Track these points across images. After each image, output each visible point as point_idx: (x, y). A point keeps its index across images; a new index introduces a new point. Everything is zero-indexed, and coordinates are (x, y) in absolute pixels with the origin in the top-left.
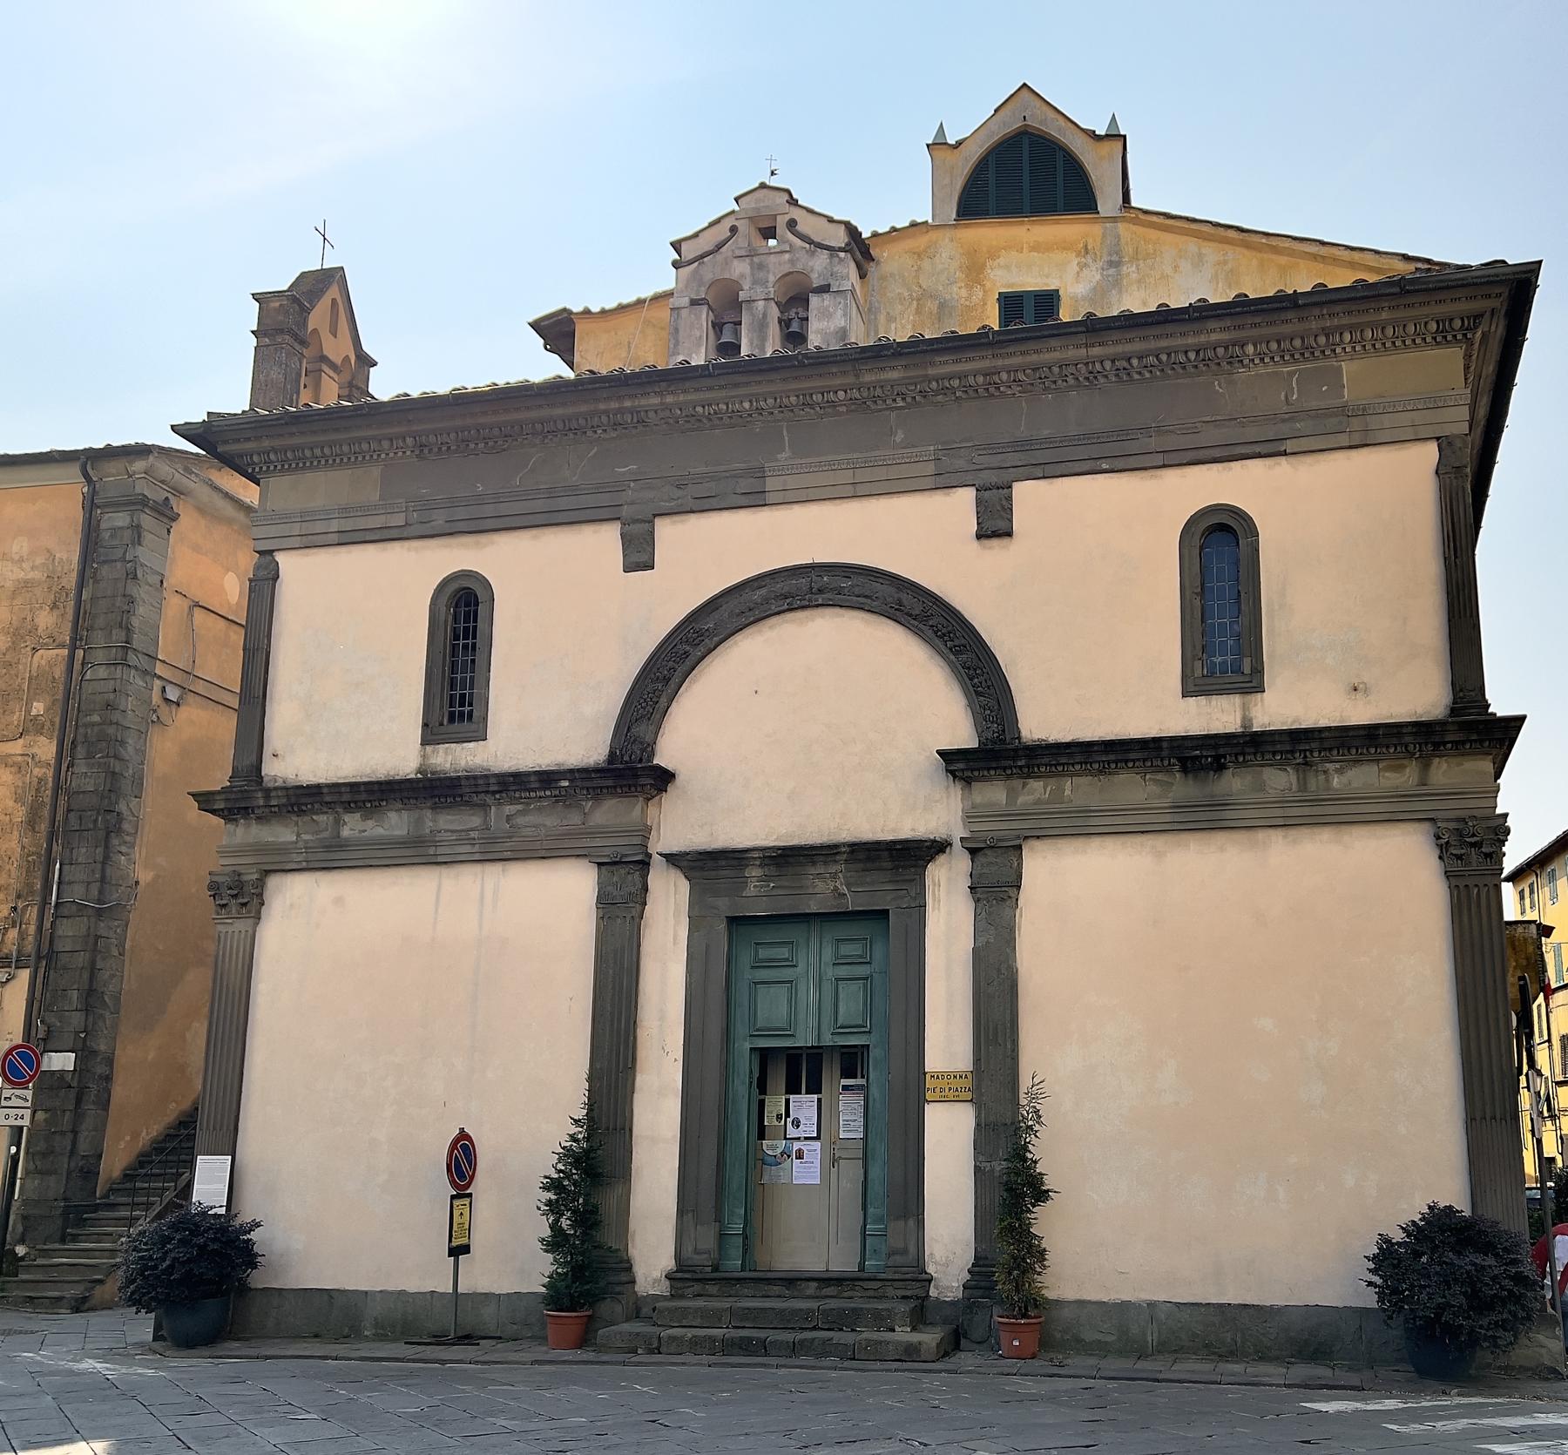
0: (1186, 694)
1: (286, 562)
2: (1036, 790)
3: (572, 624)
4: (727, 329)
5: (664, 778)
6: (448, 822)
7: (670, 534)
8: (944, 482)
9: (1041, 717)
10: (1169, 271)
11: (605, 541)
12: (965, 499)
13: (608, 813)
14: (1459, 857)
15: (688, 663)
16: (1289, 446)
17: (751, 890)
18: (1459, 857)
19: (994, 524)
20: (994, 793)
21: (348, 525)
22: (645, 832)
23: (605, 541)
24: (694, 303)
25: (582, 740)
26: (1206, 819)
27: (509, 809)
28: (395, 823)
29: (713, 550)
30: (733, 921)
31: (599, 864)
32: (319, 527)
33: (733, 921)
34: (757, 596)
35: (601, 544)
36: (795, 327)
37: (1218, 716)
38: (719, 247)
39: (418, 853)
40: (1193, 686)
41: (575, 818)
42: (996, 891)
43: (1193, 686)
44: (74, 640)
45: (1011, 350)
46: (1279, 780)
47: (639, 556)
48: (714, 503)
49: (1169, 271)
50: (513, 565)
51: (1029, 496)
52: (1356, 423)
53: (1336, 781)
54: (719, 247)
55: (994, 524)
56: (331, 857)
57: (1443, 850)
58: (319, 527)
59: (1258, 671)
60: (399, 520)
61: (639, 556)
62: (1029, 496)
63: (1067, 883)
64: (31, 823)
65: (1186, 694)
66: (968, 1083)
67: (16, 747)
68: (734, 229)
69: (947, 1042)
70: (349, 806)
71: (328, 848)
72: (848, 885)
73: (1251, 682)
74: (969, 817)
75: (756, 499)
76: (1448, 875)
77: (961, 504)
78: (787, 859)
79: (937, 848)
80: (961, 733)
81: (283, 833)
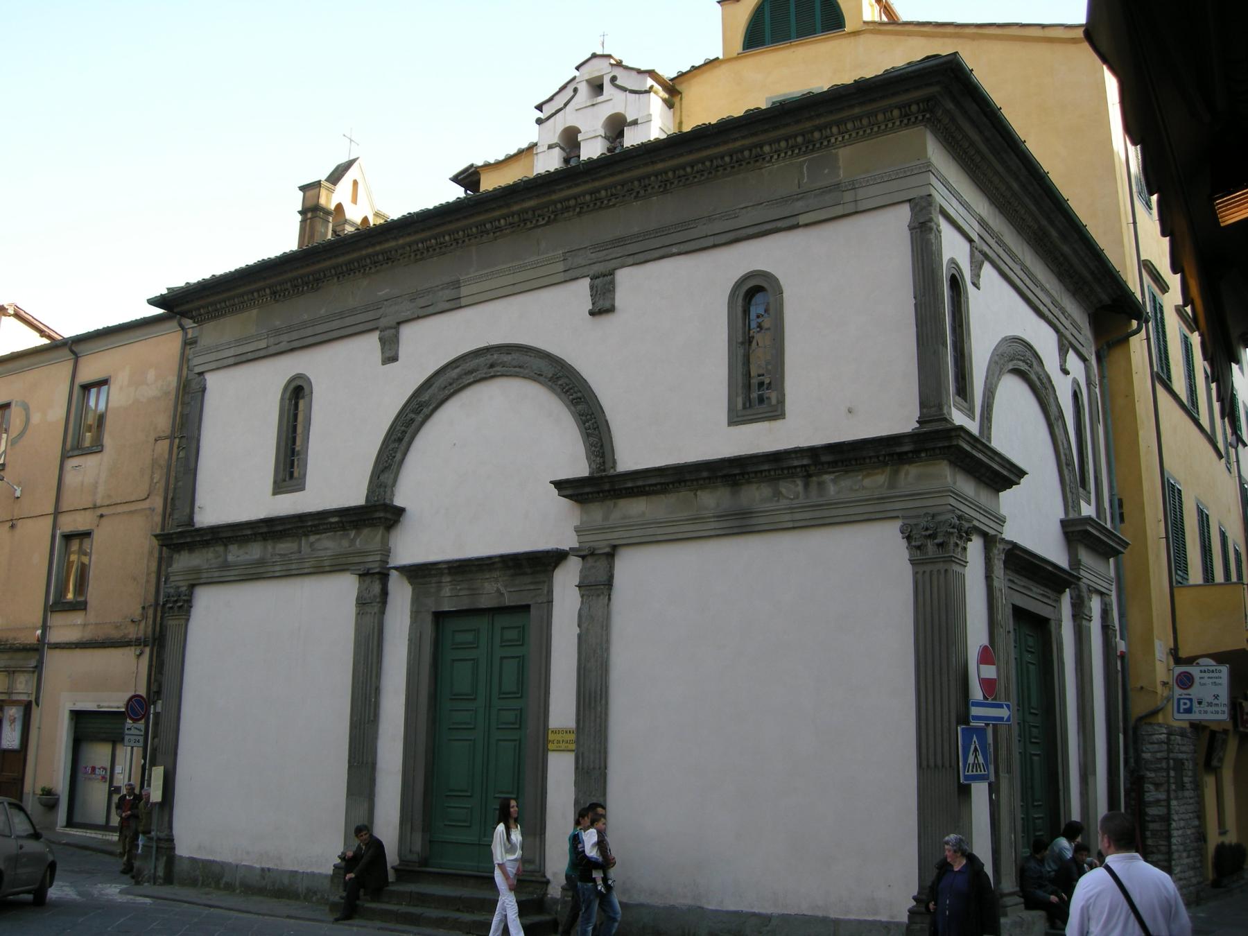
0: (731, 423)
5: (401, 511)
11: (371, 343)
12: (583, 287)
13: (367, 540)
14: (918, 548)
15: (414, 426)
16: (802, 219)
18: (918, 548)
19: (602, 307)
20: (597, 513)
22: (386, 552)
23: (371, 343)
26: (740, 524)
29: (433, 342)
30: (439, 617)
31: (360, 575)
40: (736, 418)
41: (345, 543)
42: (598, 588)
43: (736, 418)
45: (602, 174)
46: (792, 489)
48: (431, 310)
51: (629, 281)
52: (848, 196)
53: (832, 489)
55: (602, 307)
59: (781, 401)
62: (629, 281)
66: (573, 737)
72: (506, 586)
73: (776, 412)
75: (455, 305)
76: (913, 562)
77: (579, 293)
80: (580, 468)
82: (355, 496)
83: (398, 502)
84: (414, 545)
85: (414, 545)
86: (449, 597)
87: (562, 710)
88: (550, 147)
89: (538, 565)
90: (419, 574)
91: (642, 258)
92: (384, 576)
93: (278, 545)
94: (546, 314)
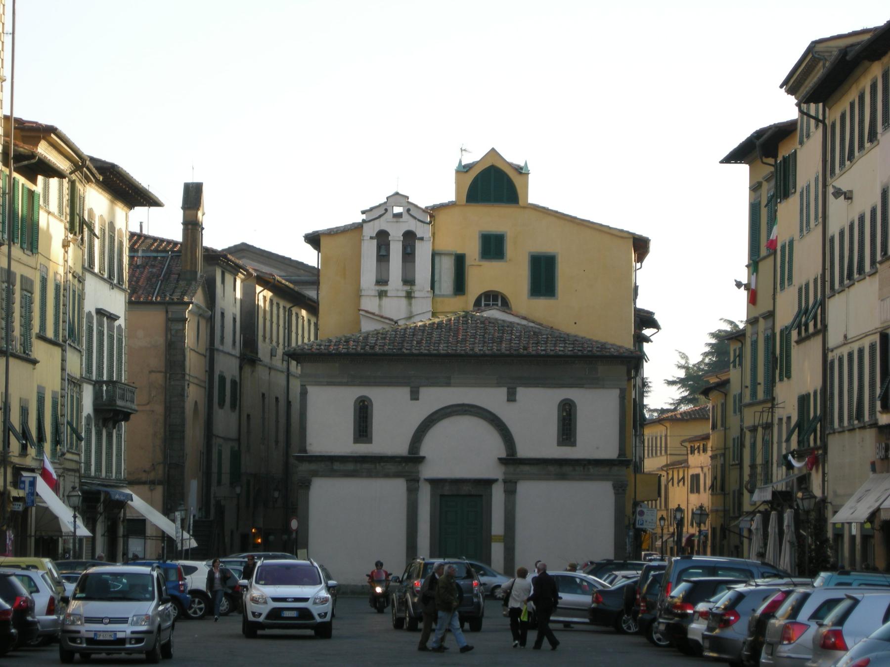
1: (310, 389)
3: (397, 414)
4: (383, 247)
5: (424, 458)
7: (424, 392)
8: (498, 385)
9: (524, 451)
11: (405, 392)
19: (512, 397)
24: (371, 238)
25: (401, 448)
26: (563, 477)
28: (350, 466)
29: (436, 397)
33: (442, 496)
34: (449, 410)
36: (409, 250)
38: (380, 216)
42: (510, 491)
47: (415, 396)
51: (521, 392)
53: (592, 470)
54: (380, 216)
55: (512, 397)
56: (332, 474)
57: (614, 487)
60: (345, 380)
61: (415, 396)
62: (521, 392)
63: (531, 492)
67: (148, 408)
69: (497, 527)
73: (573, 444)
74: (505, 473)
75: (448, 384)
77: (502, 392)
79: (496, 481)
83: (422, 454)
84: (429, 471)
85: (429, 471)
86: (447, 490)
89: (488, 483)
92: (418, 481)
94: (492, 397)
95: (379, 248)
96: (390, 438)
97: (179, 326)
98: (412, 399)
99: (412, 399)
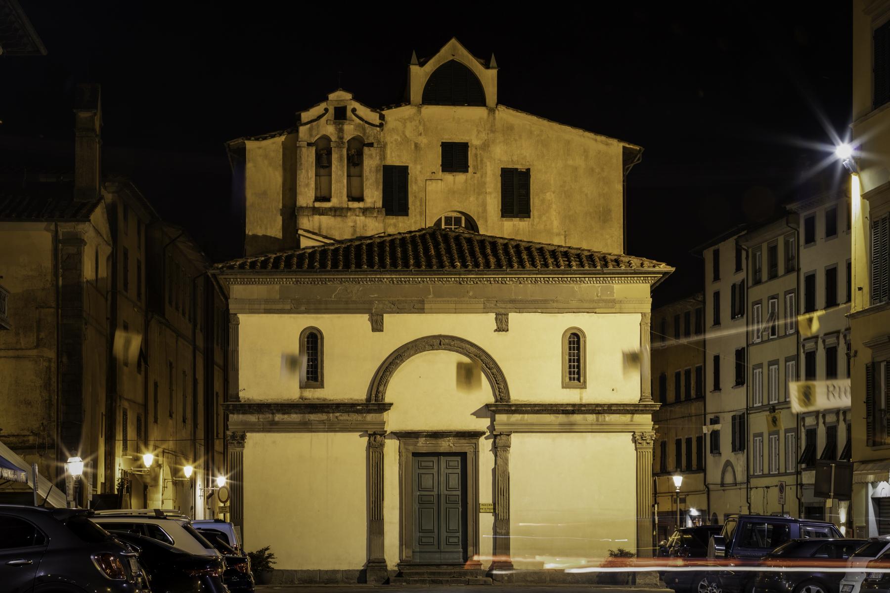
2: (516, 418)
6: (313, 417)
8: (486, 310)
9: (517, 395)
10: (517, 138)
16: (597, 310)
17: (420, 444)
19: (502, 327)
21: (268, 307)
22: (383, 423)
24: (309, 145)
27: (338, 414)
28: (295, 417)
29: (404, 327)
30: (415, 454)
32: (256, 306)
35: (362, 321)
37: (572, 396)
39: (305, 427)
40: (564, 386)
43: (564, 386)
44: (58, 305)
46: (591, 418)
47: (377, 326)
49: (517, 138)
50: (328, 324)
51: (513, 317)
55: (502, 327)
56: (272, 427)
58: (256, 306)
59: (585, 382)
60: (288, 307)
61: (377, 326)
62: (513, 317)
64: (47, 385)
65: (563, 387)
68: (326, 110)
70: (278, 411)
71: (271, 425)
78: (436, 435)
81: (252, 418)
82: (359, 393)
83: (387, 400)
86: (422, 445)
87: (485, 495)
88: (309, 145)
90: (403, 436)
91: (520, 310)
93: (311, 414)
94: (476, 326)
95: (318, 157)
96: (345, 382)
97: (72, 250)
98: (374, 330)
99: (374, 330)
